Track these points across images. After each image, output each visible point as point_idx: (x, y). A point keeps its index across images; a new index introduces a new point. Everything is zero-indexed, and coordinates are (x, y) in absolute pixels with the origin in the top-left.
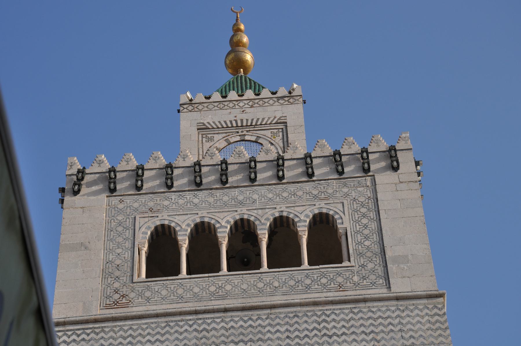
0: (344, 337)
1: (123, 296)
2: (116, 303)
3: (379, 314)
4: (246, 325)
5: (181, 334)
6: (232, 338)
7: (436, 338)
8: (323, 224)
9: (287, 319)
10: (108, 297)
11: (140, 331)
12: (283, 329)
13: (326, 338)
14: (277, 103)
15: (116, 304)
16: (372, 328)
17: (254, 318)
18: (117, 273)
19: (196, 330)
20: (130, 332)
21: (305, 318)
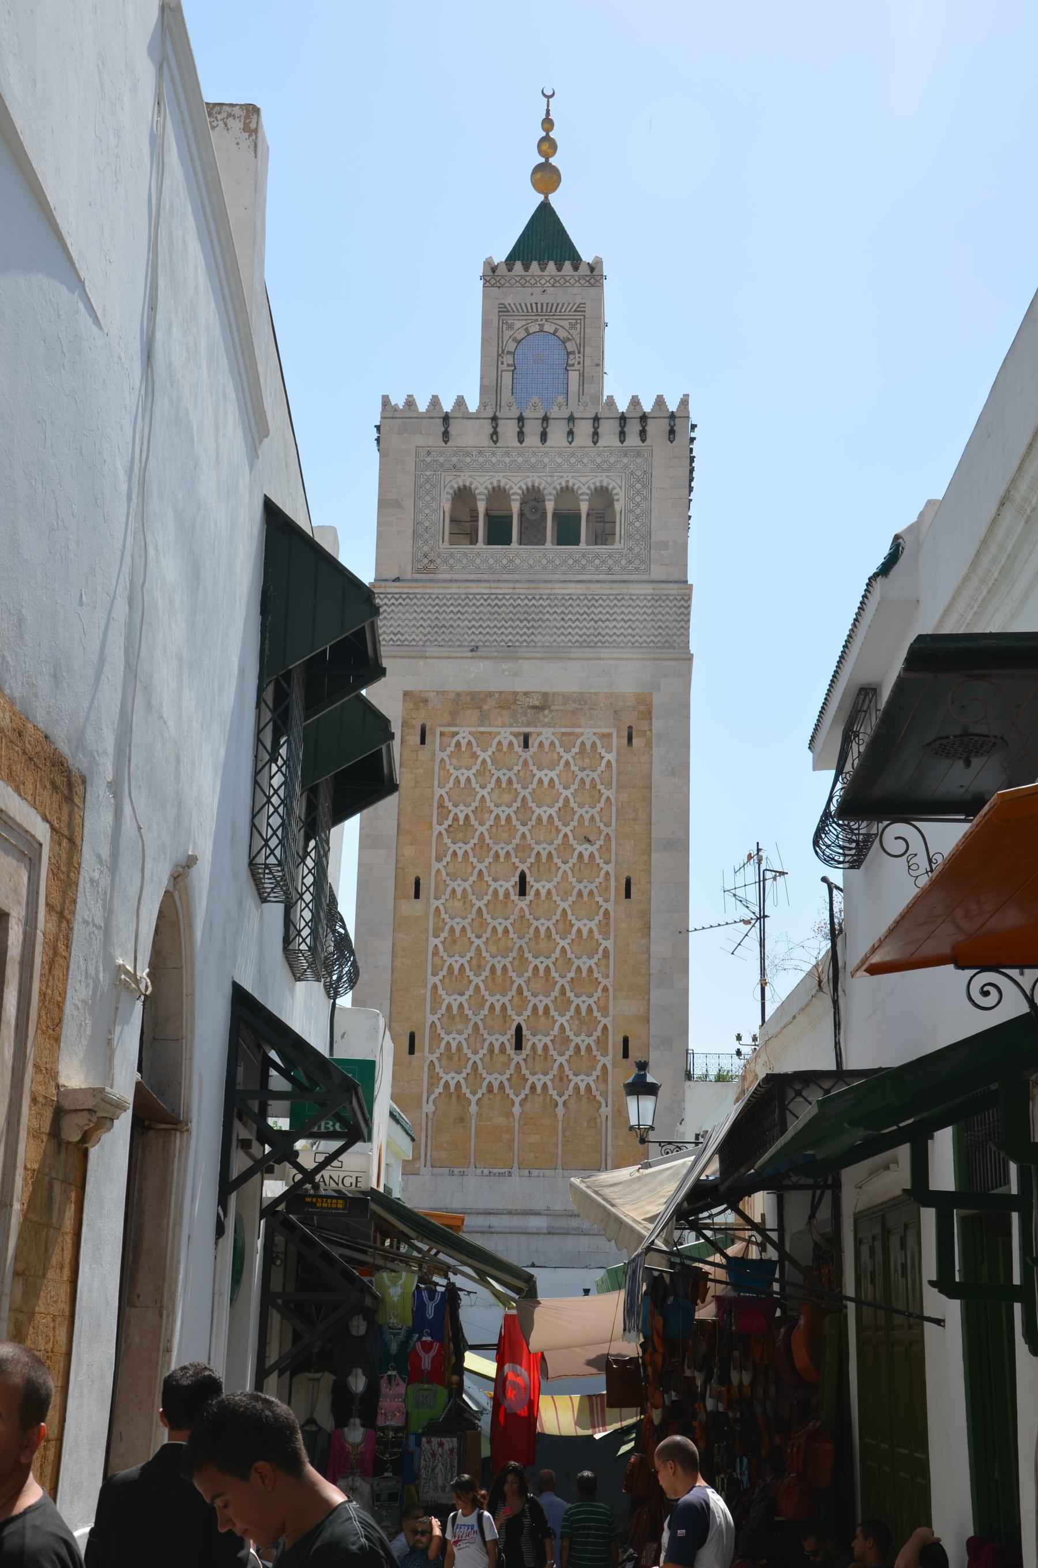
0: (607, 623)
1: (431, 561)
2: (425, 568)
3: (638, 602)
4: (530, 604)
5: (478, 607)
6: (518, 615)
7: (679, 629)
8: (603, 496)
9: (563, 601)
10: (419, 561)
11: (445, 601)
12: (559, 611)
13: (592, 623)
14: (577, 284)
15: (425, 570)
16: (630, 616)
17: (537, 597)
18: (426, 536)
19: (489, 605)
20: (437, 601)
21: (578, 602)
